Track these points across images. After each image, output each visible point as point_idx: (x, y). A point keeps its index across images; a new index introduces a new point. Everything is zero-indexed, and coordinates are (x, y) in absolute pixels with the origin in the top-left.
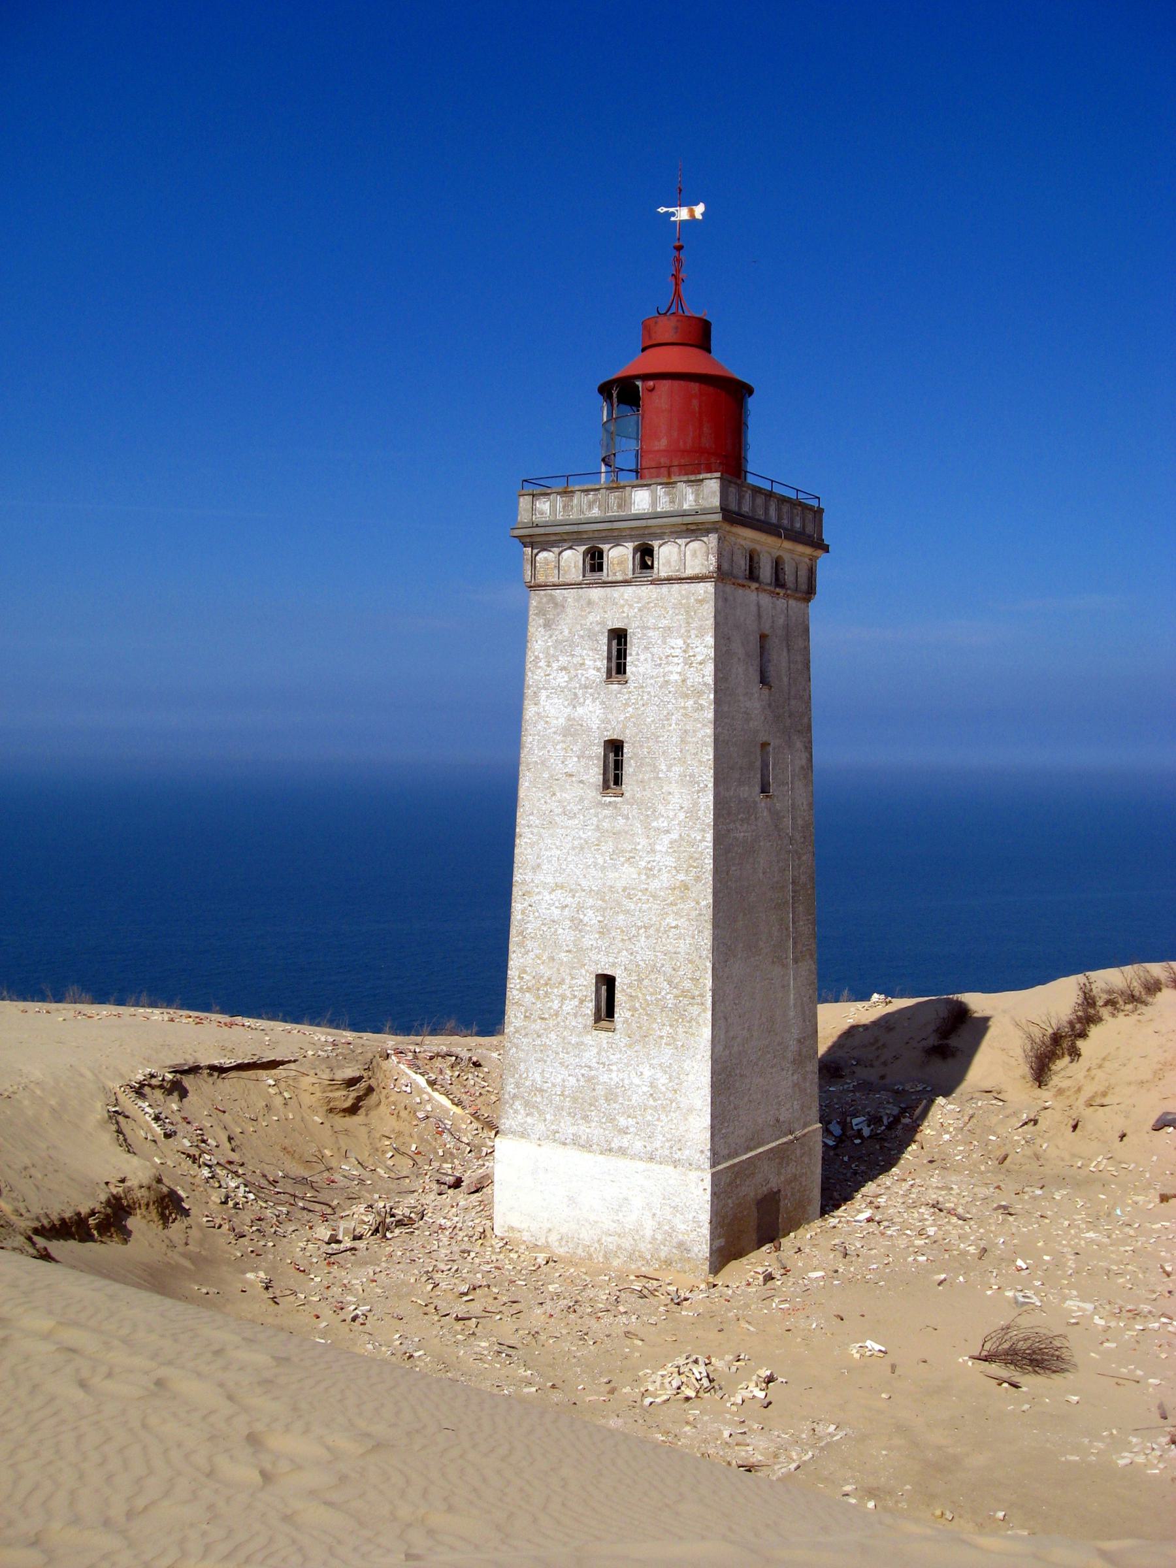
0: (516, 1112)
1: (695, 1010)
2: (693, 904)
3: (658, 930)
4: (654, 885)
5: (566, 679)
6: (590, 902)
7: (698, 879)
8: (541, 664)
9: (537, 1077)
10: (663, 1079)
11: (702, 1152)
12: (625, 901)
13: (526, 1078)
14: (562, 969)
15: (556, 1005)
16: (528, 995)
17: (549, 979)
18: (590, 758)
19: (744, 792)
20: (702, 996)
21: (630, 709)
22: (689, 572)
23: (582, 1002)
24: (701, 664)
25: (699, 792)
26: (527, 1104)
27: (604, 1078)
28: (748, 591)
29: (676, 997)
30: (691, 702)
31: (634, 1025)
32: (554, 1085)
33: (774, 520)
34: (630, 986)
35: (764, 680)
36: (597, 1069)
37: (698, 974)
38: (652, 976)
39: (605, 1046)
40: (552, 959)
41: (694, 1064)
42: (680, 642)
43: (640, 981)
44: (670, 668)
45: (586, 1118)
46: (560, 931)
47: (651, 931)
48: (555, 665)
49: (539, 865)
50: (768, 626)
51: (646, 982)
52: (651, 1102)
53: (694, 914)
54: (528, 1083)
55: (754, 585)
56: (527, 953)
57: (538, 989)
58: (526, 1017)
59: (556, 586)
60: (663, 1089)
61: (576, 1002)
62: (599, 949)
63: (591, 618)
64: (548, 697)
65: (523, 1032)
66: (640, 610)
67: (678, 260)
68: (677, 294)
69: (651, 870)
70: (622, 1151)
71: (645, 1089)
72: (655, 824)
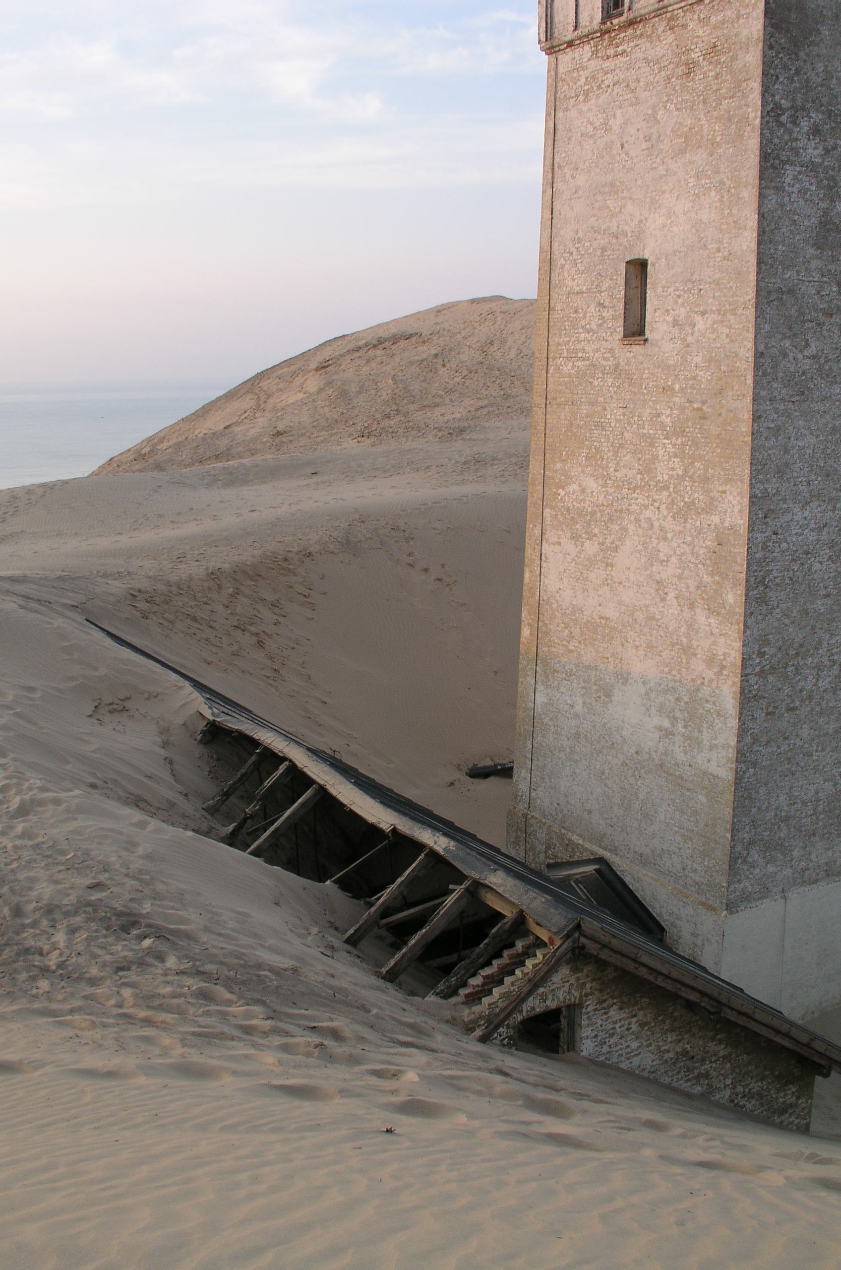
8: (784, 119)
16: (771, 679)
17: (801, 646)
32: (804, 804)
46: (817, 566)
48: (805, 124)
49: (786, 465)
58: (768, 714)
64: (795, 178)
65: (764, 739)
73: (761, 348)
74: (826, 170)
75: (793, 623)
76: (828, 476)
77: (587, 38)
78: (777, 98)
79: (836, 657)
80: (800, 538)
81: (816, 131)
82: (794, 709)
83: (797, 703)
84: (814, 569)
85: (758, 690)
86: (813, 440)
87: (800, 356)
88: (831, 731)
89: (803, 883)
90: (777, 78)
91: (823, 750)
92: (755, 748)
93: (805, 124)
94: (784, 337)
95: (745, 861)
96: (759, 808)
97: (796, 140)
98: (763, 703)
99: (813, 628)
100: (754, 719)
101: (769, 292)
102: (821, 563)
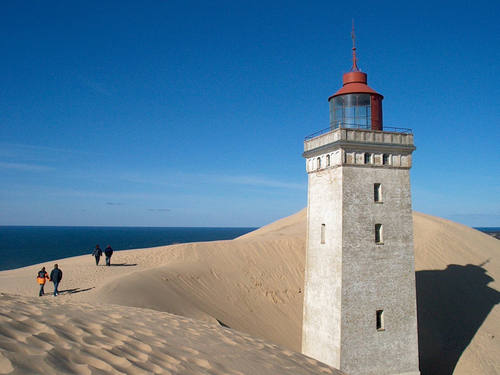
1: (412, 317)
2: (409, 280)
3: (398, 291)
7: (410, 272)
8: (349, 195)
9: (355, 353)
10: (402, 343)
11: (416, 365)
13: (351, 356)
16: (350, 323)
20: (413, 312)
21: (384, 213)
22: (402, 166)
23: (371, 322)
24: (407, 197)
25: (409, 242)
26: (351, 366)
27: (381, 348)
29: (405, 314)
30: (404, 211)
31: (391, 327)
32: (362, 356)
34: (389, 313)
36: (378, 346)
37: (412, 304)
38: (397, 308)
39: (381, 336)
42: (400, 190)
43: (393, 310)
44: (397, 199)
45: (375, 365)
46: (362, 297)
47: (396, 292)
48: (354, 196)
51: (395, 310)
53: (409, 284)
56: (349, 307)
57: (354, 321)
60: (402, 347)
61: (369, 322)
63: (367, 179)
64: (352, 207)
65: (349, 338)
66: (385, 177)
69: (394, 270)
71: (396, 349)
72: (395, 254)
73: (344, 246)
74: (361, 205)
75: (356, 310)
76: (364, 275)
77: (315, 171)
78: (347, 191)
79: (369, 319)
80: (357, 290)
81: (358, 197)
82: (357, 331)
83: (358, 330)
84: (361, 297)
85: (346, 326)
86: (359, 267)
87: (355, 248)
88: (369, 338)
90: (347, 186)
91: (367, 342)
92: (346, 340)
93: (354, 196)
94: (350, 243)
95: (345, 368)
96: (348, 356)
97: (352, 199)
99: (362, 312)
100: (345, 333)
101: (346, 234)
102: (363, 296)
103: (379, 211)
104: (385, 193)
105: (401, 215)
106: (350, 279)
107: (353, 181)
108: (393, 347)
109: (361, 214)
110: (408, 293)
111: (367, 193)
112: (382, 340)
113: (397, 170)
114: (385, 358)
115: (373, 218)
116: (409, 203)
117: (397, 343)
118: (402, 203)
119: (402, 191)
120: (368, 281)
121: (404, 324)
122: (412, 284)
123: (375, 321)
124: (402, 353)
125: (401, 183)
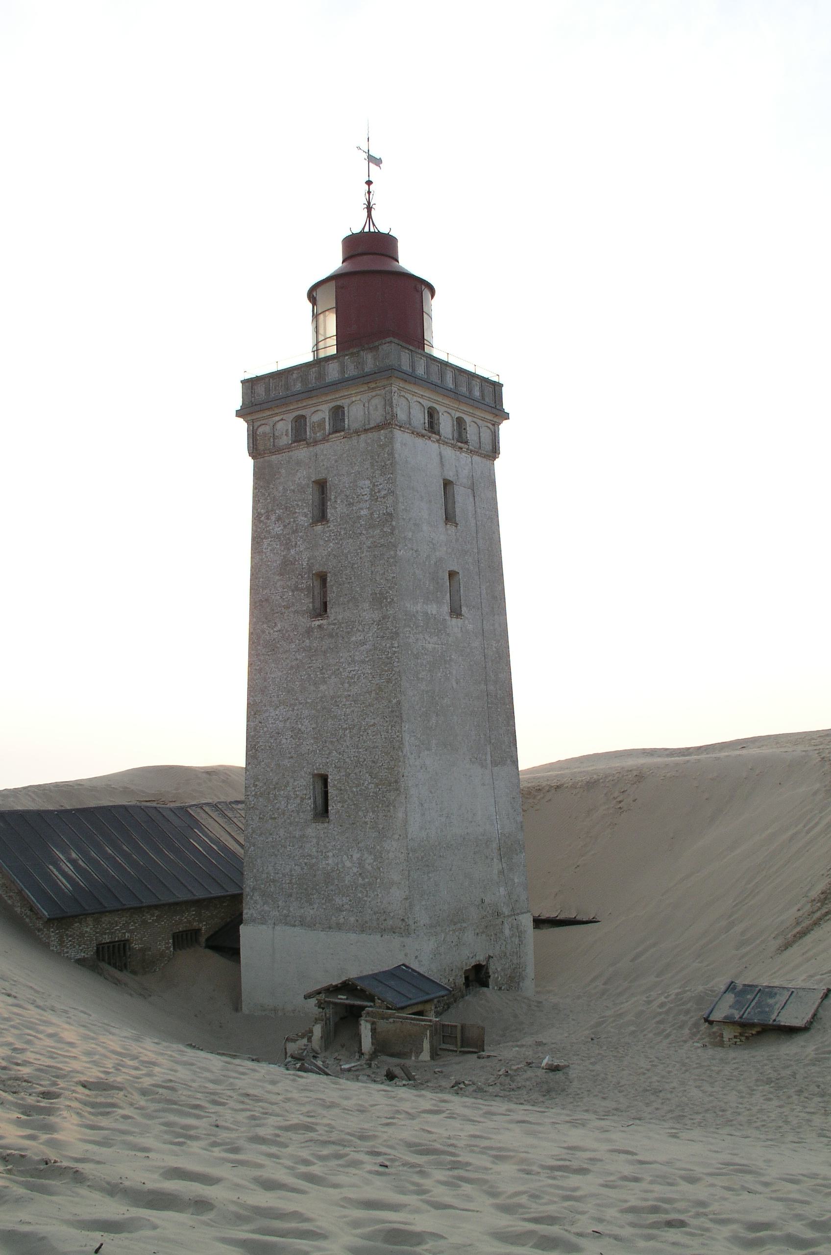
0: (256, 902)
4: (355, 690)
5: (282, 527)
6: (306, 712)
9: (270, 868)
10: (369, 859)
12: (334, 708)
14: (286, 773)
15: (283, 805)
17: (277, 784)
18: (302, 590)
19: (432, 609)
20: (396, 782)
23: (302, 799)
24: (384, 497)
28: (429, 442)
29: (377, 785)
32: (284, 875)
33: (451, 385)
34: (339, 781)
35: (450, 518)
37: (392, 763)
38: (357, 771)
40: (278, 765)
41: (393, 843)
42: (367, 482)
46: (284, 741)
48: (273, 518)
50: (451, 474)
52: (360, 881)
54: (264, 876)
55: (435, 437)
56: (259, 763)
59: (272, 453)
60: (370, 868)
61: (298, 801)
62: (315, 751)
64: (269, 545)
66: (336, 461)
67: (369, 192)
68: (369, 216)
69: (352, 678)
70: (339, 927)
71: (355, 870)
72: (354, 639)
81: (279, 519)
82: (275, 818)
86: (280, 674)
89: (286, 924)
93: (273, 518)
94: (263, 623)
95: (251, 898)
98: (257, 812)
99: (284, 775)
103: (321, 542)
104: (336, 497)
105: (369, 543)
106: (261, 701)
107: (272, 486)
108: (348, 864)
109: (284, 557)
110: (384, 734)
111: (298, 505)
112: (325, 846)
113: (363, 437)
114: (331, 887)
115: (309, 559)
116: (390, 510)
117: (358, 855)
118: (372, 514)
119: (374, 485)
120: (295, 705)
121: (373, 812)
122: (392, 711)
123: (310, 798)
124: (370, 884)
125: (372, 465)
